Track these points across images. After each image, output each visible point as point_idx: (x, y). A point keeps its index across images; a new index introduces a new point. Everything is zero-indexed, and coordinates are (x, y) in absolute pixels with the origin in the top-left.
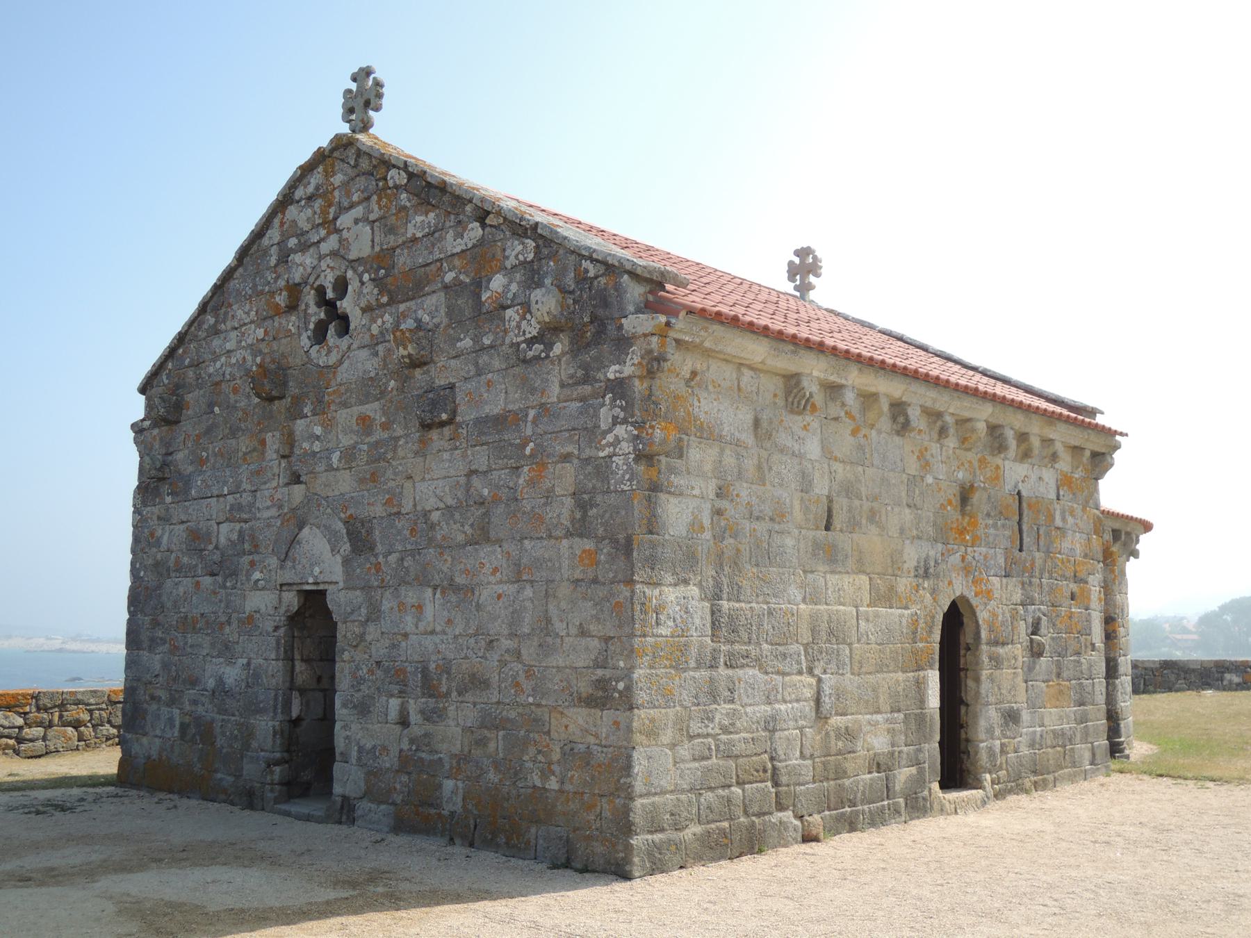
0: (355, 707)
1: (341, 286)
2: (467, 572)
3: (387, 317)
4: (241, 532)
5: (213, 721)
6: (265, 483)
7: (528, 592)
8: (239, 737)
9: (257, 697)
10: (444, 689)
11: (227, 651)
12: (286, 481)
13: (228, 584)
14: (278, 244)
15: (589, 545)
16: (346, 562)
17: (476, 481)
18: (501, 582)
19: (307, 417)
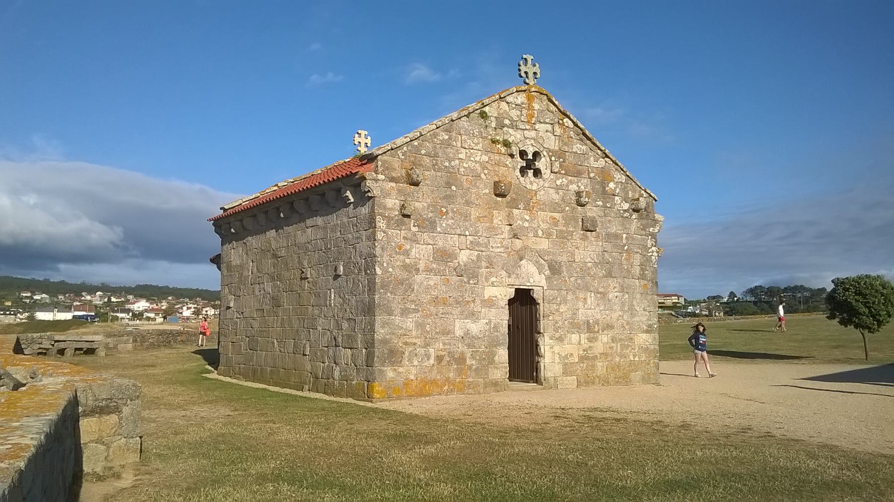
0: (557, 339)
2: (603, 287)
3: (564, 180)
4: (478, 256)
5: (463, 353)
6: (497, 235)
8: (487, 359)
9: (497, 339)
10: (596, 330)
11: (473, 316)
12: (510, 236)
13: (471, 282)
14: (495, 117)
15: (646, 282)
16: (548, 278)
18: (616, 292)
19: (520, 209)
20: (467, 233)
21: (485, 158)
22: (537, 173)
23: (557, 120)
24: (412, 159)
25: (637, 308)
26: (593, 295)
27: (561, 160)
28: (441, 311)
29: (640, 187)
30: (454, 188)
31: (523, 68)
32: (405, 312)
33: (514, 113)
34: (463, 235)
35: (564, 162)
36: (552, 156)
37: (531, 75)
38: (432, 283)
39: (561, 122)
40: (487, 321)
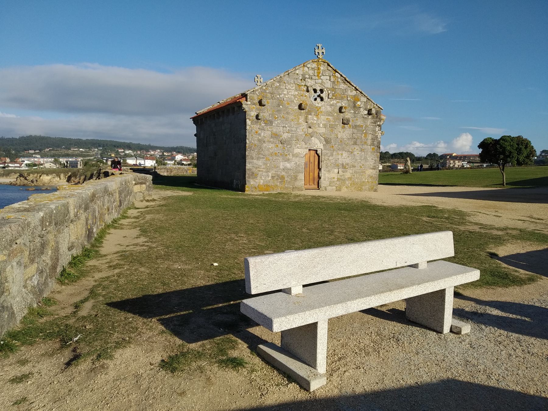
1: (322, 91)
4: (291, 136)
7: (363, 153)
11: (288, 160)
14: (302, 75)
17: (354, 135)
20: (287, 126)
21: (297, 93)
22: (322, 99)
23: (332, 74)
24: (262, 95)
25: (369, 159)
26: (346, 152)
27: (334, 92)
28: (274, 158)
29: (374, 103)
30: (281, 107)
31: (317, 51)
32: (258, 159)
33: (311, 72)
34: (285, 127)
35: (335, 93)
36: (329, 91)
37: (320, 54)
38: (270, 147)
39: (334, 75)
40: (295, 163)
